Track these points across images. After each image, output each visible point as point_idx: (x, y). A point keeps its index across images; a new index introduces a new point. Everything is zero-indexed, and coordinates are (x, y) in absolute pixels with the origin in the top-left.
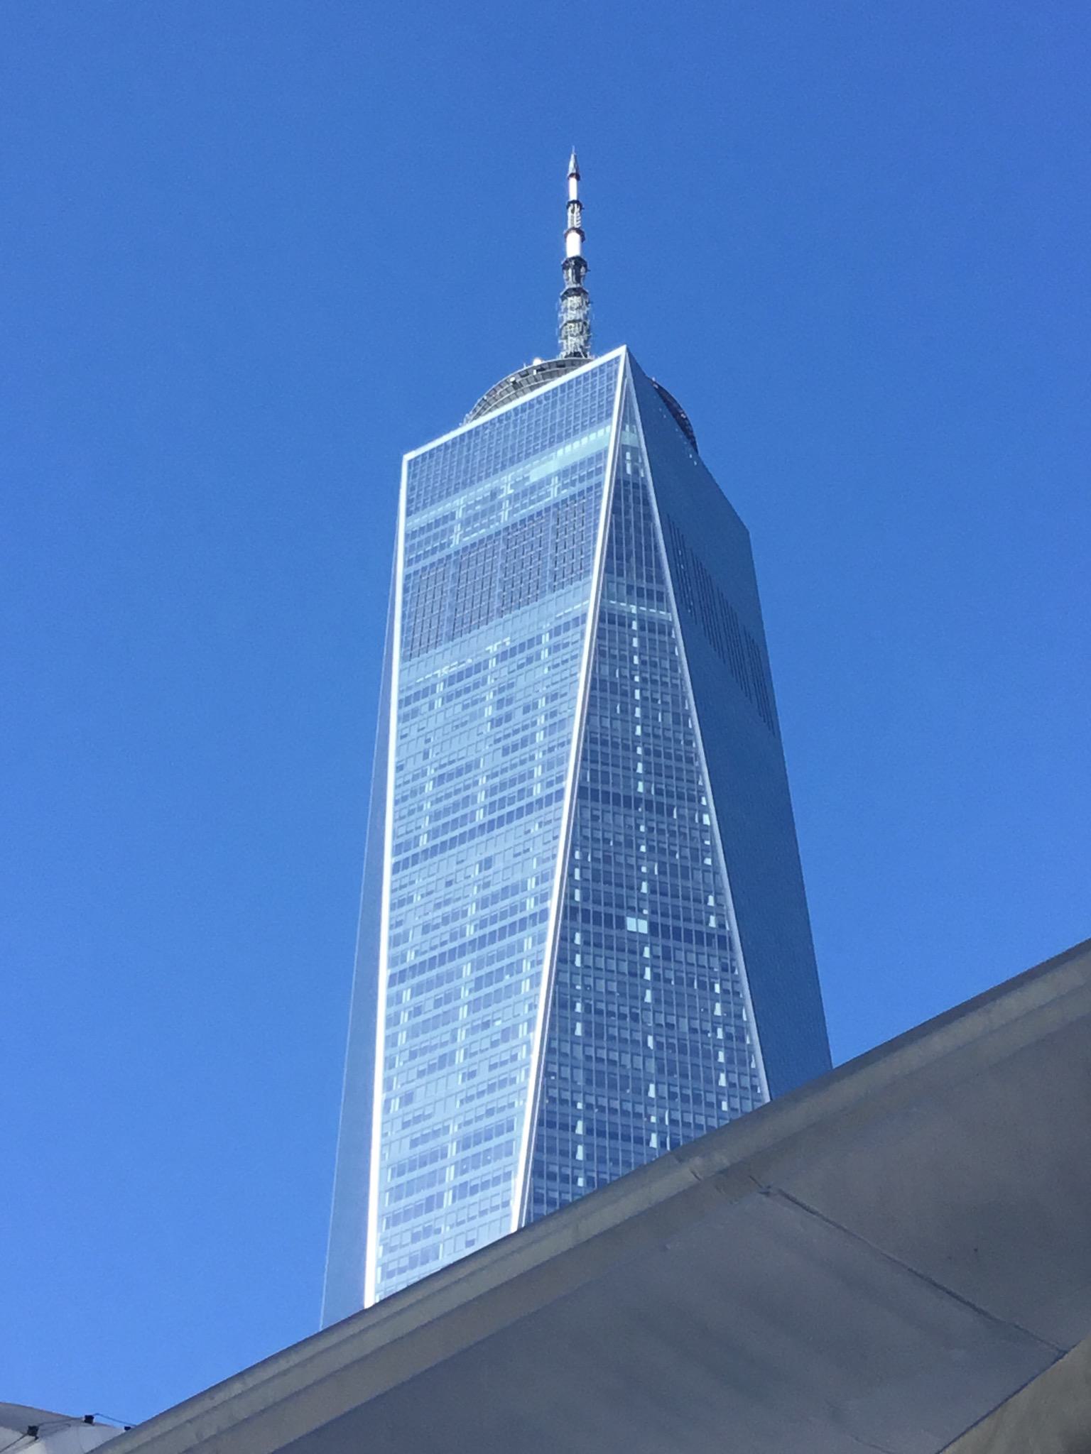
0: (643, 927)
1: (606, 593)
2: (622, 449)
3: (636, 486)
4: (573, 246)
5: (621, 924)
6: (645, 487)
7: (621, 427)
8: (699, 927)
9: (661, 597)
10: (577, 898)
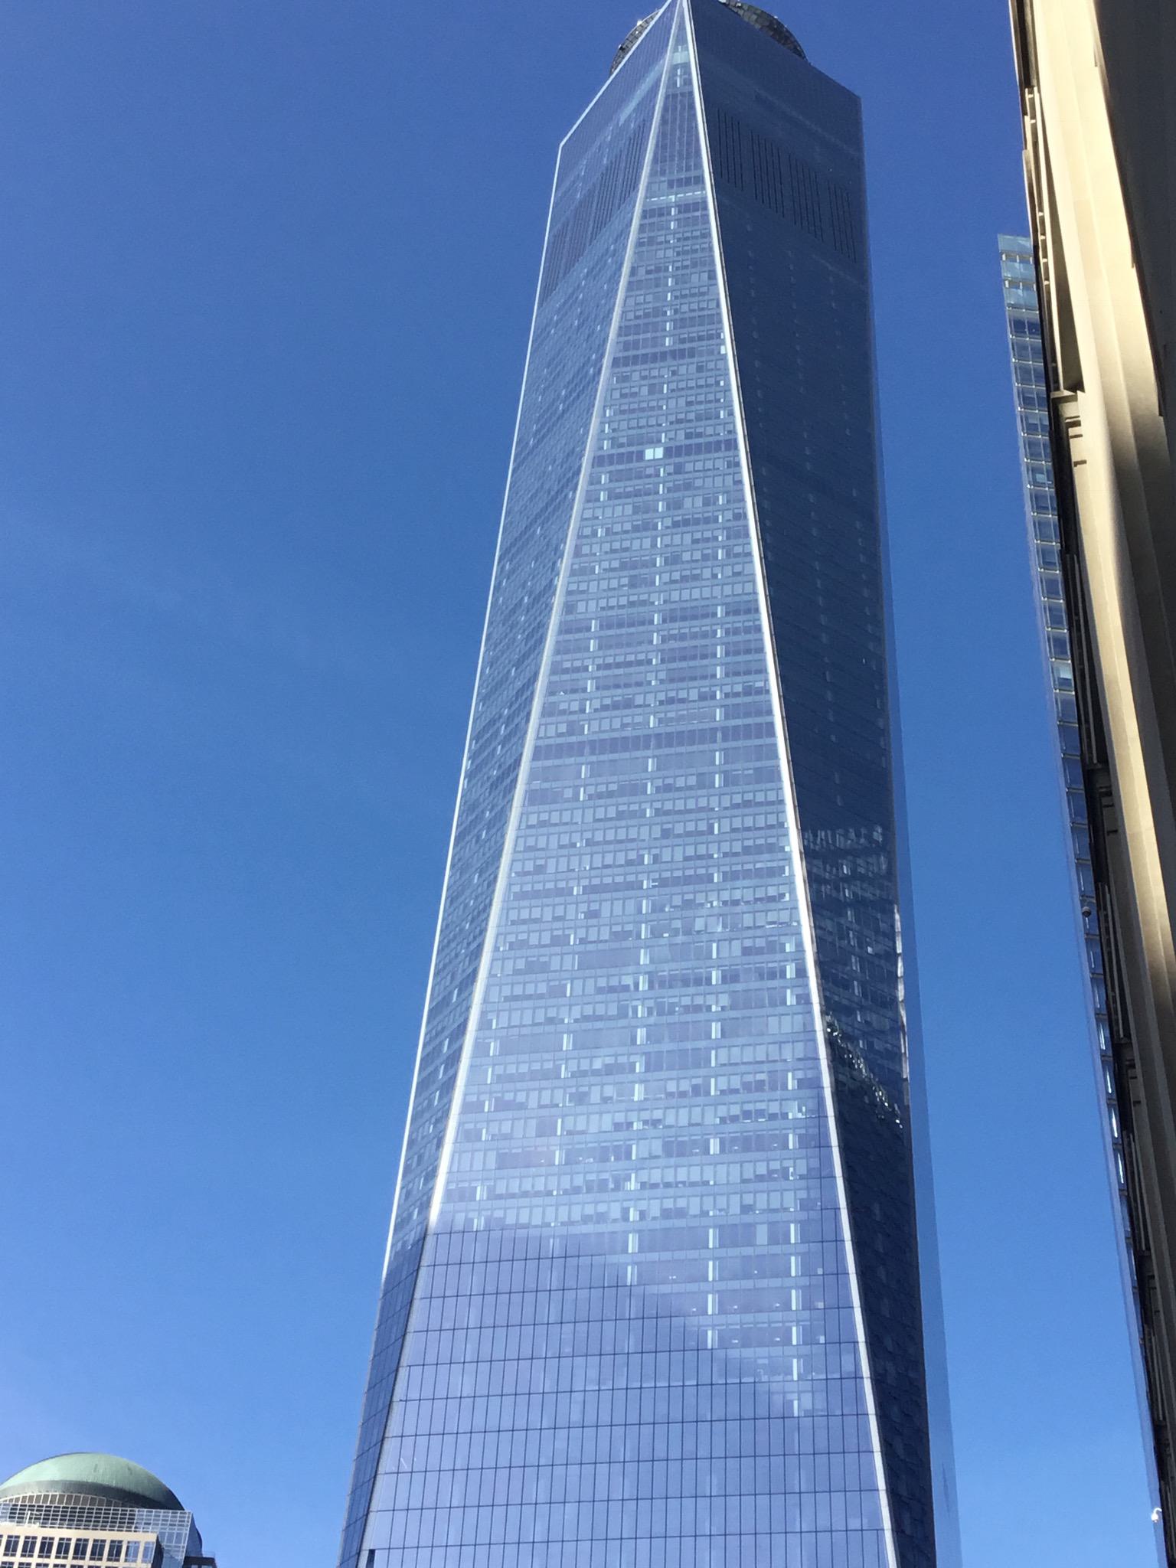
0: (659, 453)
1: (650, 193)
2: (674, 68)
3: (682, 94)
5: (640, 455)
6: (691, 93)
7: (675, 50)
8: (711, 439)
9: (700, 180)
10: (606, 444)
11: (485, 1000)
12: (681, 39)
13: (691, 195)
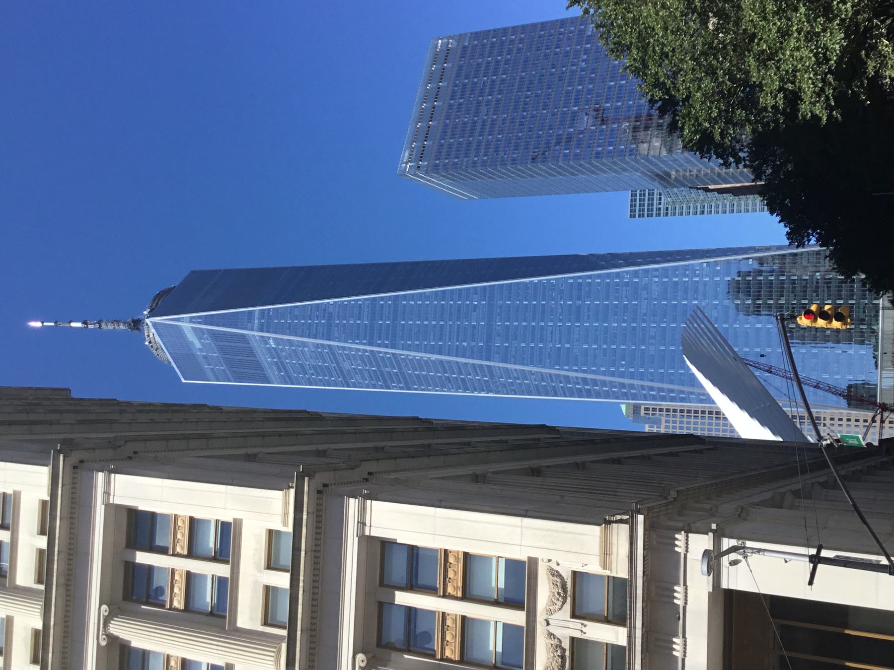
1: (252, 330)
4: (79, 325)
11: (576, 371)
12: (178, 320)
13: (257, 315)
